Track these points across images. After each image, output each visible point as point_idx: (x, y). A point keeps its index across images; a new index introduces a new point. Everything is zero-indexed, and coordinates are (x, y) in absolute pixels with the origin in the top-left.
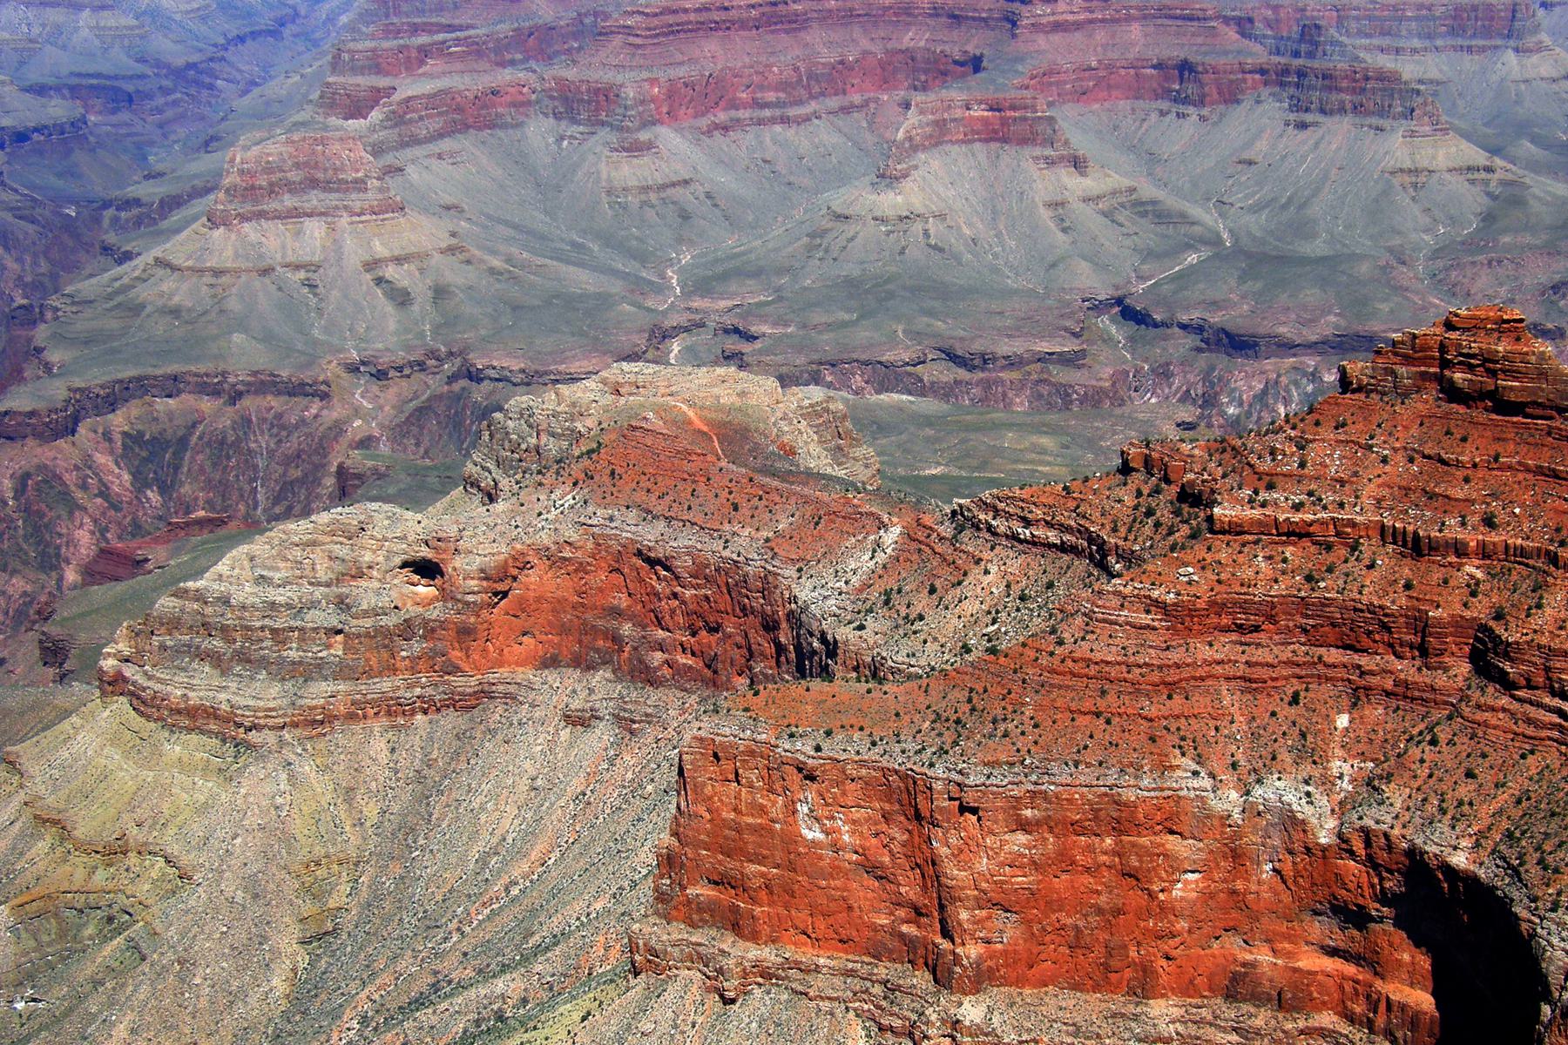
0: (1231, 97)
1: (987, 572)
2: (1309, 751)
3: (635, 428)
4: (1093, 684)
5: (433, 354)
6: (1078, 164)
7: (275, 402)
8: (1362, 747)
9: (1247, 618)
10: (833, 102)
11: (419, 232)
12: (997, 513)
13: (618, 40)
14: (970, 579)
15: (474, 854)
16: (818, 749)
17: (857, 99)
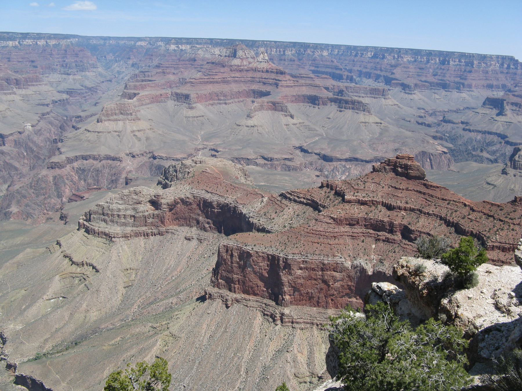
0: (324, 104)
1: (289, 209)
2: (366, 253)
3: (203, 172)
4: (317, 236)
5: (146, 152)
6: (292, 117)
7: (110, 162)
8: (378, 253)
9: (352, 223)
10: (236, 100)
11: (143, 125)
12: (291, 194)
13: (189, 84)
14: (285, 210)
15: (164, 269)
16: (252, 249)
17: (242, 99)
